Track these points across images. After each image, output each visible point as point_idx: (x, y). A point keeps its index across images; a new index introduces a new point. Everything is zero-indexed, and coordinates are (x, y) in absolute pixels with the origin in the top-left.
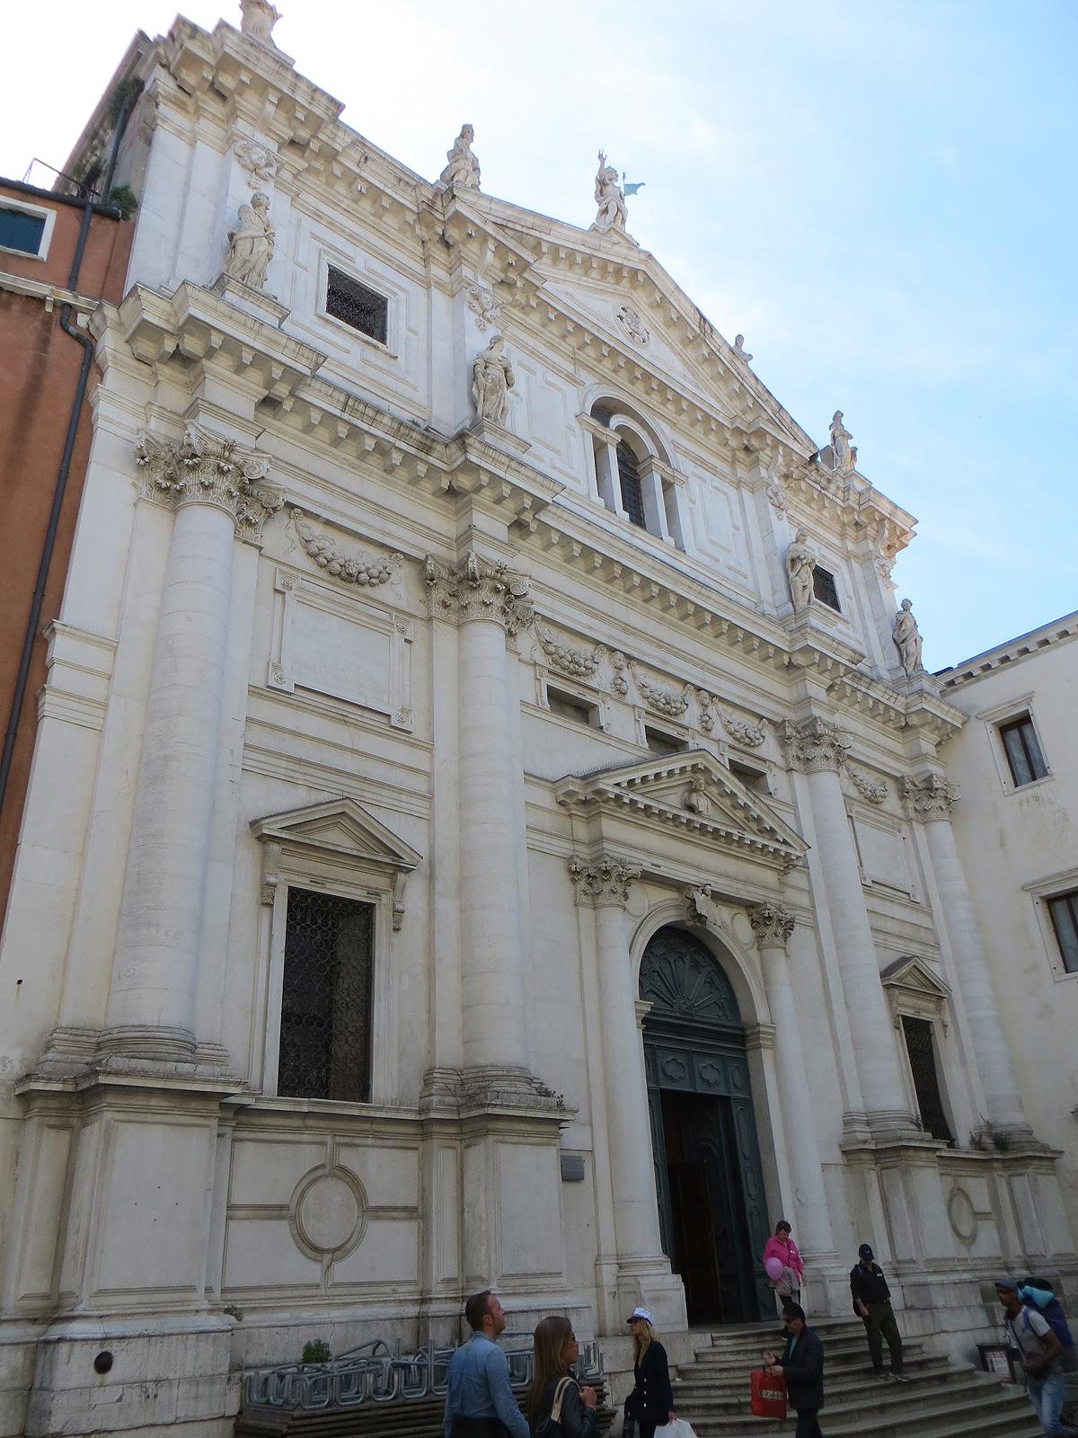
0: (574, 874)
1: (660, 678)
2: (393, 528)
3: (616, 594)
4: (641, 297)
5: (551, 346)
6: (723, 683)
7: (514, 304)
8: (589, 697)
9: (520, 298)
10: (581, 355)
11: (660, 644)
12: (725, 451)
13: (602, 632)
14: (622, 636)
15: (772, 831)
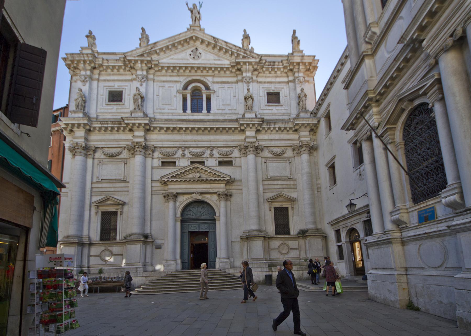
0: (164, 197)
1: (197, 149)
2: (121, 143)
3: (182, 134)
4: (198, 43)
5: (171, 76)
6: (218, 143)
7: (156, 71)
8: (173, 160)
9: (156, 69)
10: (179, 73)
11: (195, 141)
12: (233, 74)
13: (177, 144)
14: (184, 143)
15: (219, 175)
